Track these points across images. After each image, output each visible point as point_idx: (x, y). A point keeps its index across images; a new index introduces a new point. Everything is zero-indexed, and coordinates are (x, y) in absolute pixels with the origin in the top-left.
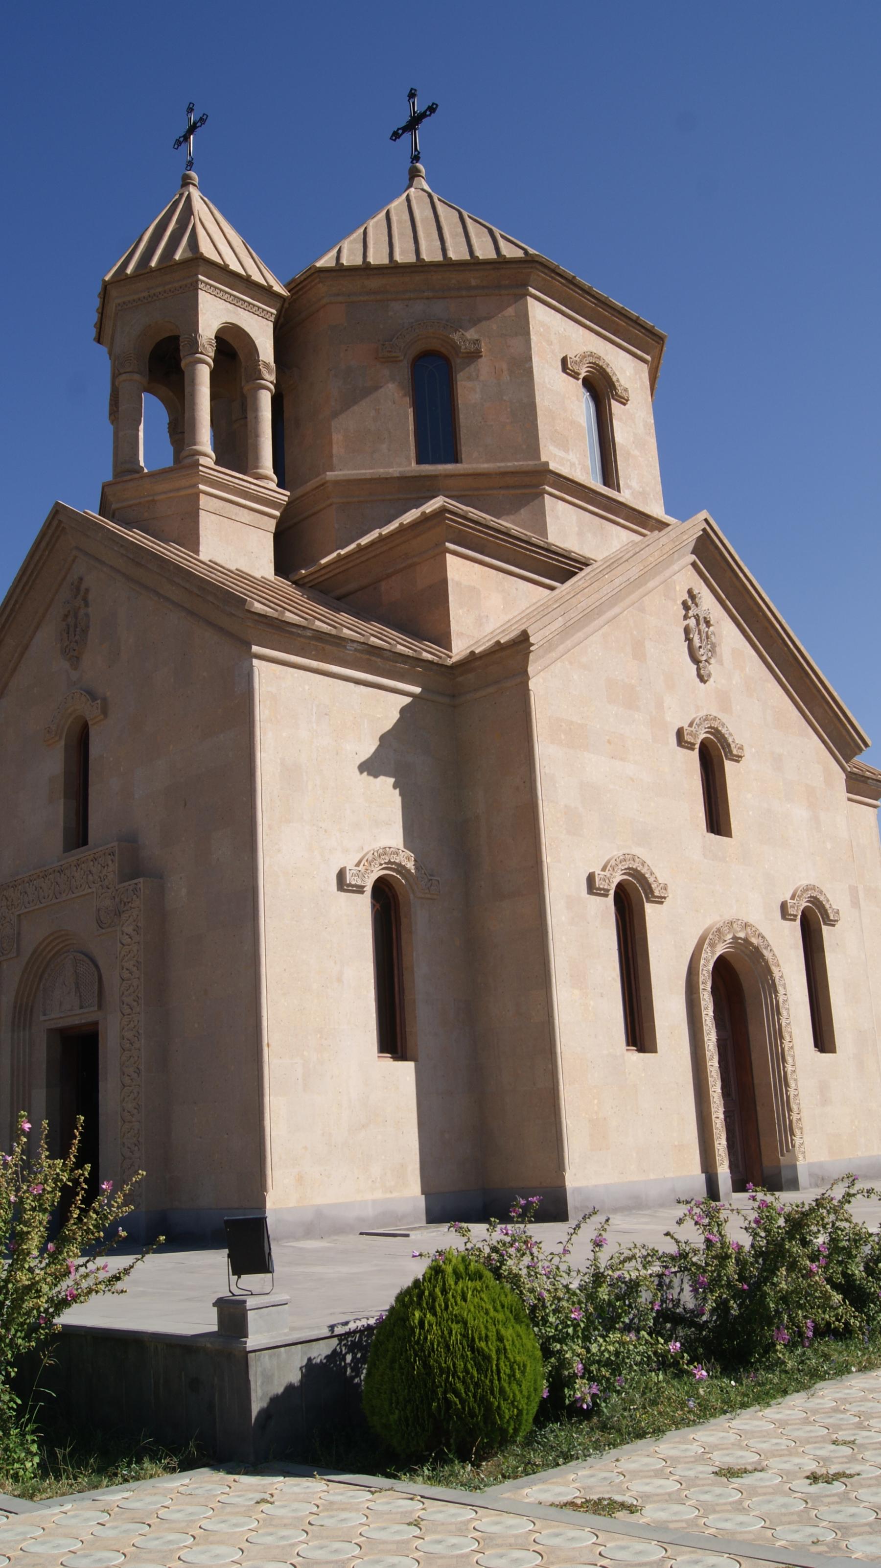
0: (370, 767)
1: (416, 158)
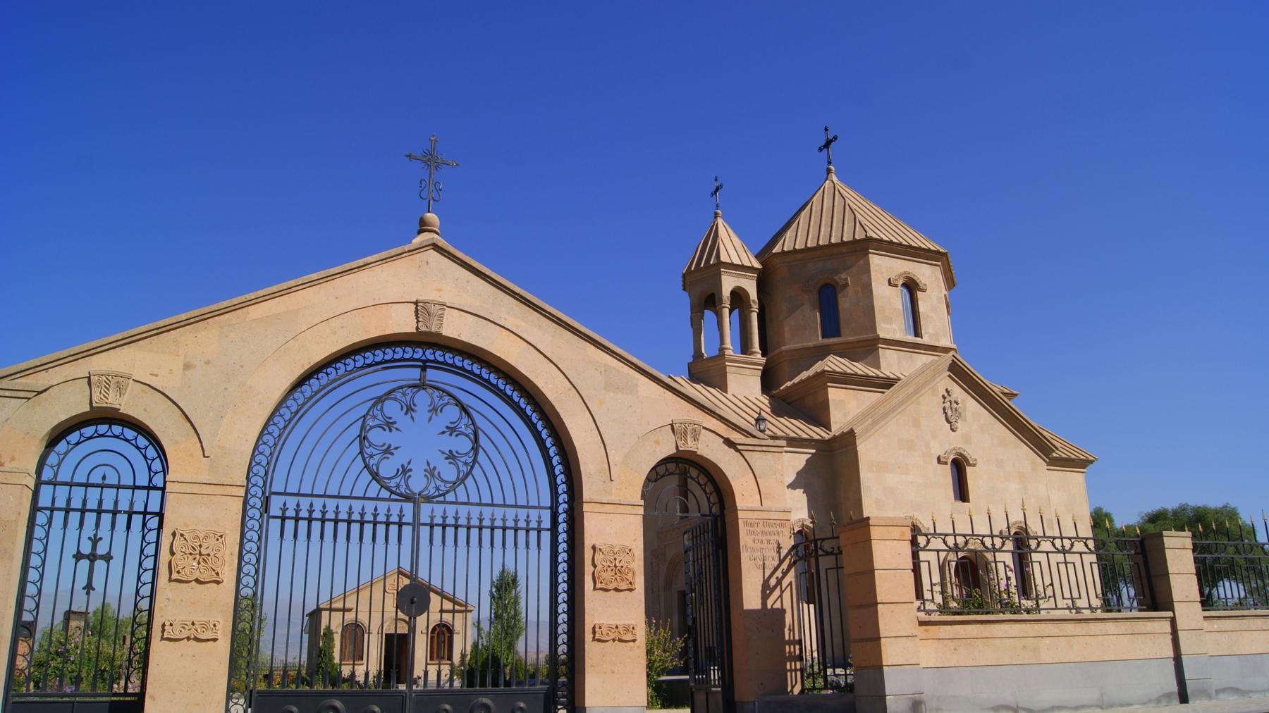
0: (792, 486)
1: (830, 163)
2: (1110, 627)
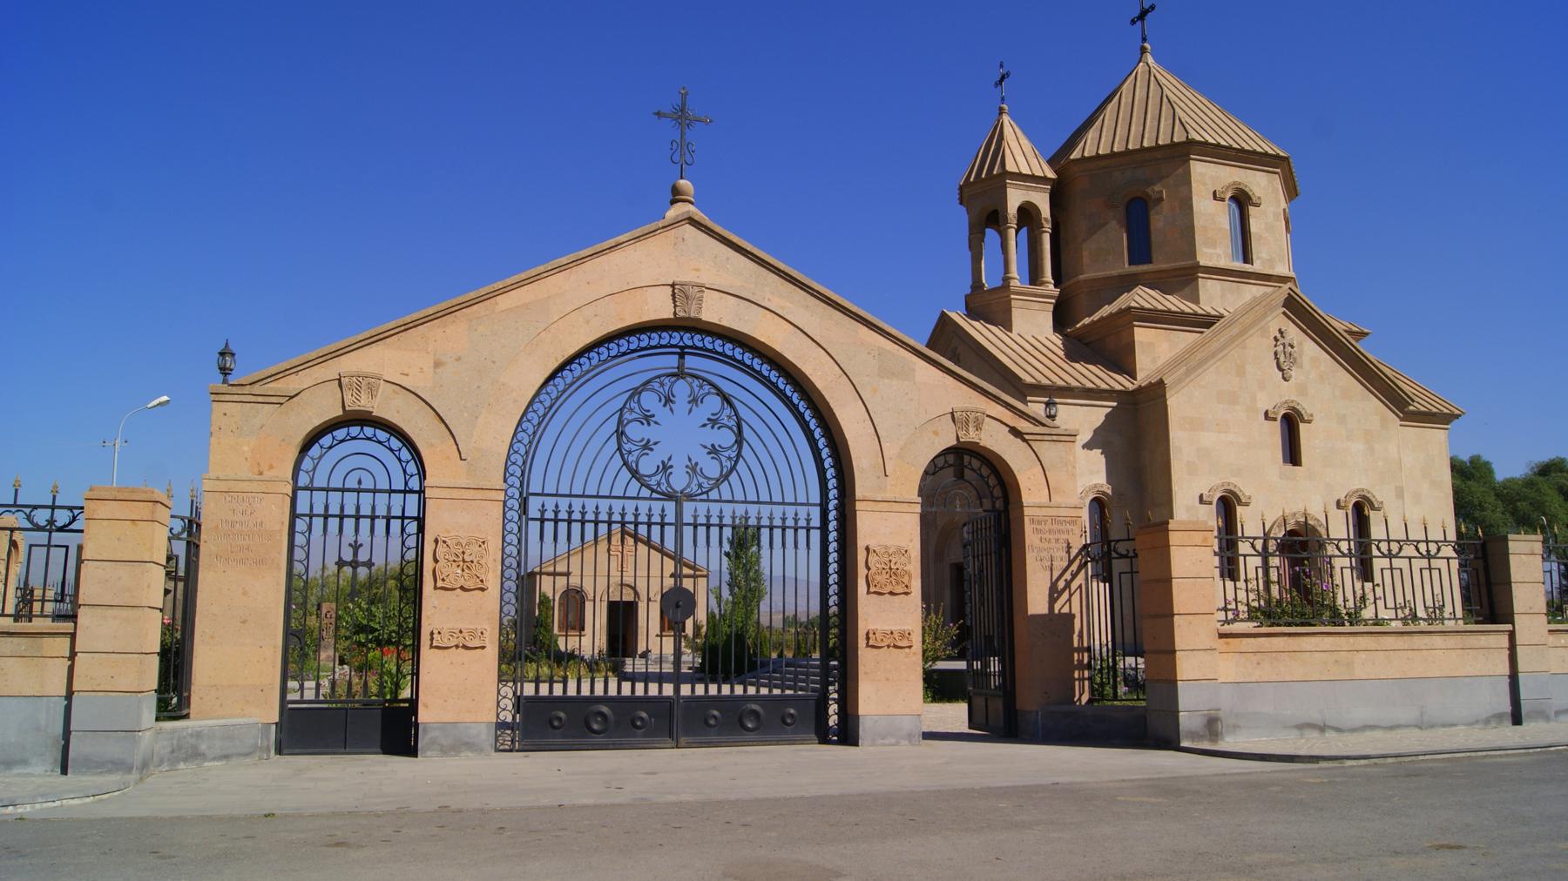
0: (1088, 446)
1: (1144, 40)
2: (1437, 640)
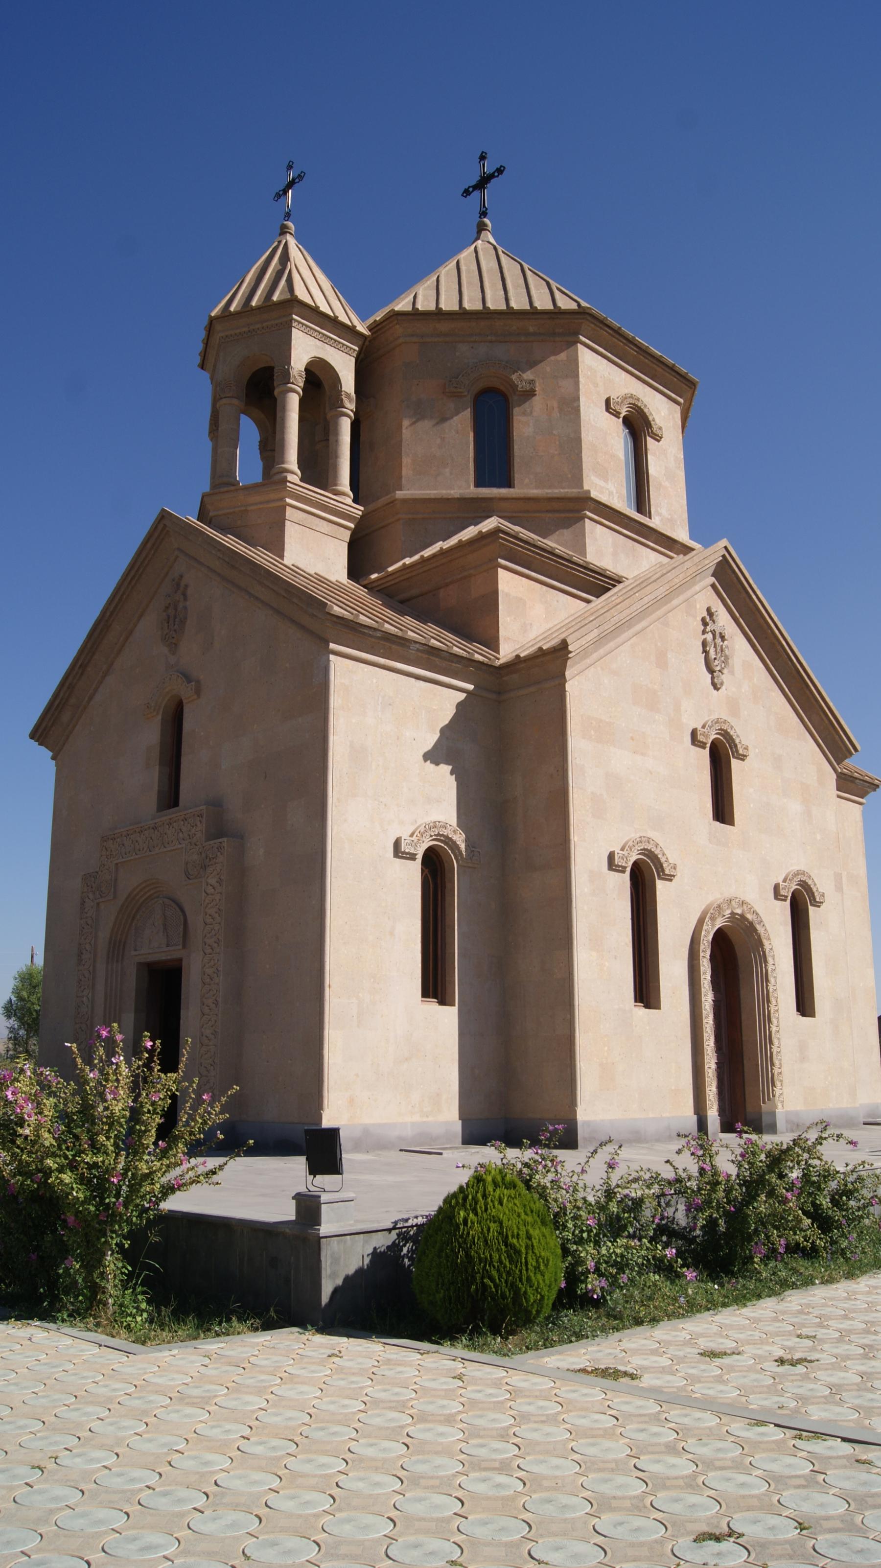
1: (484, 214)
